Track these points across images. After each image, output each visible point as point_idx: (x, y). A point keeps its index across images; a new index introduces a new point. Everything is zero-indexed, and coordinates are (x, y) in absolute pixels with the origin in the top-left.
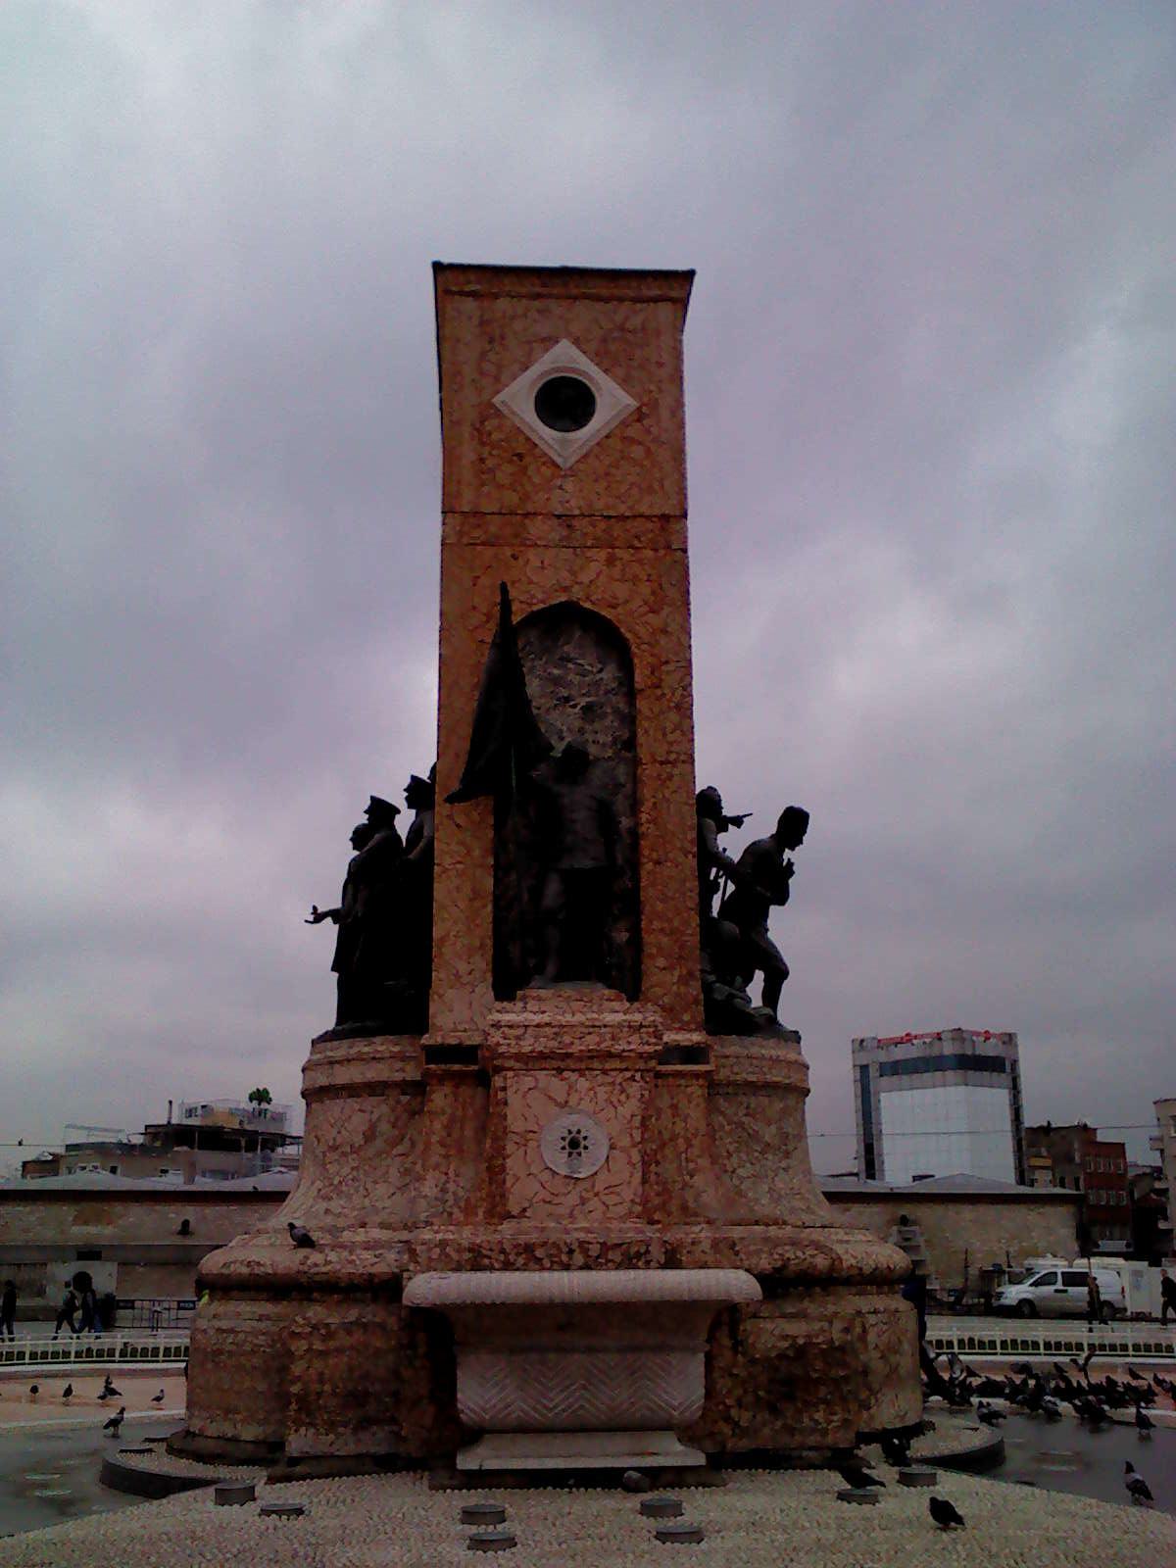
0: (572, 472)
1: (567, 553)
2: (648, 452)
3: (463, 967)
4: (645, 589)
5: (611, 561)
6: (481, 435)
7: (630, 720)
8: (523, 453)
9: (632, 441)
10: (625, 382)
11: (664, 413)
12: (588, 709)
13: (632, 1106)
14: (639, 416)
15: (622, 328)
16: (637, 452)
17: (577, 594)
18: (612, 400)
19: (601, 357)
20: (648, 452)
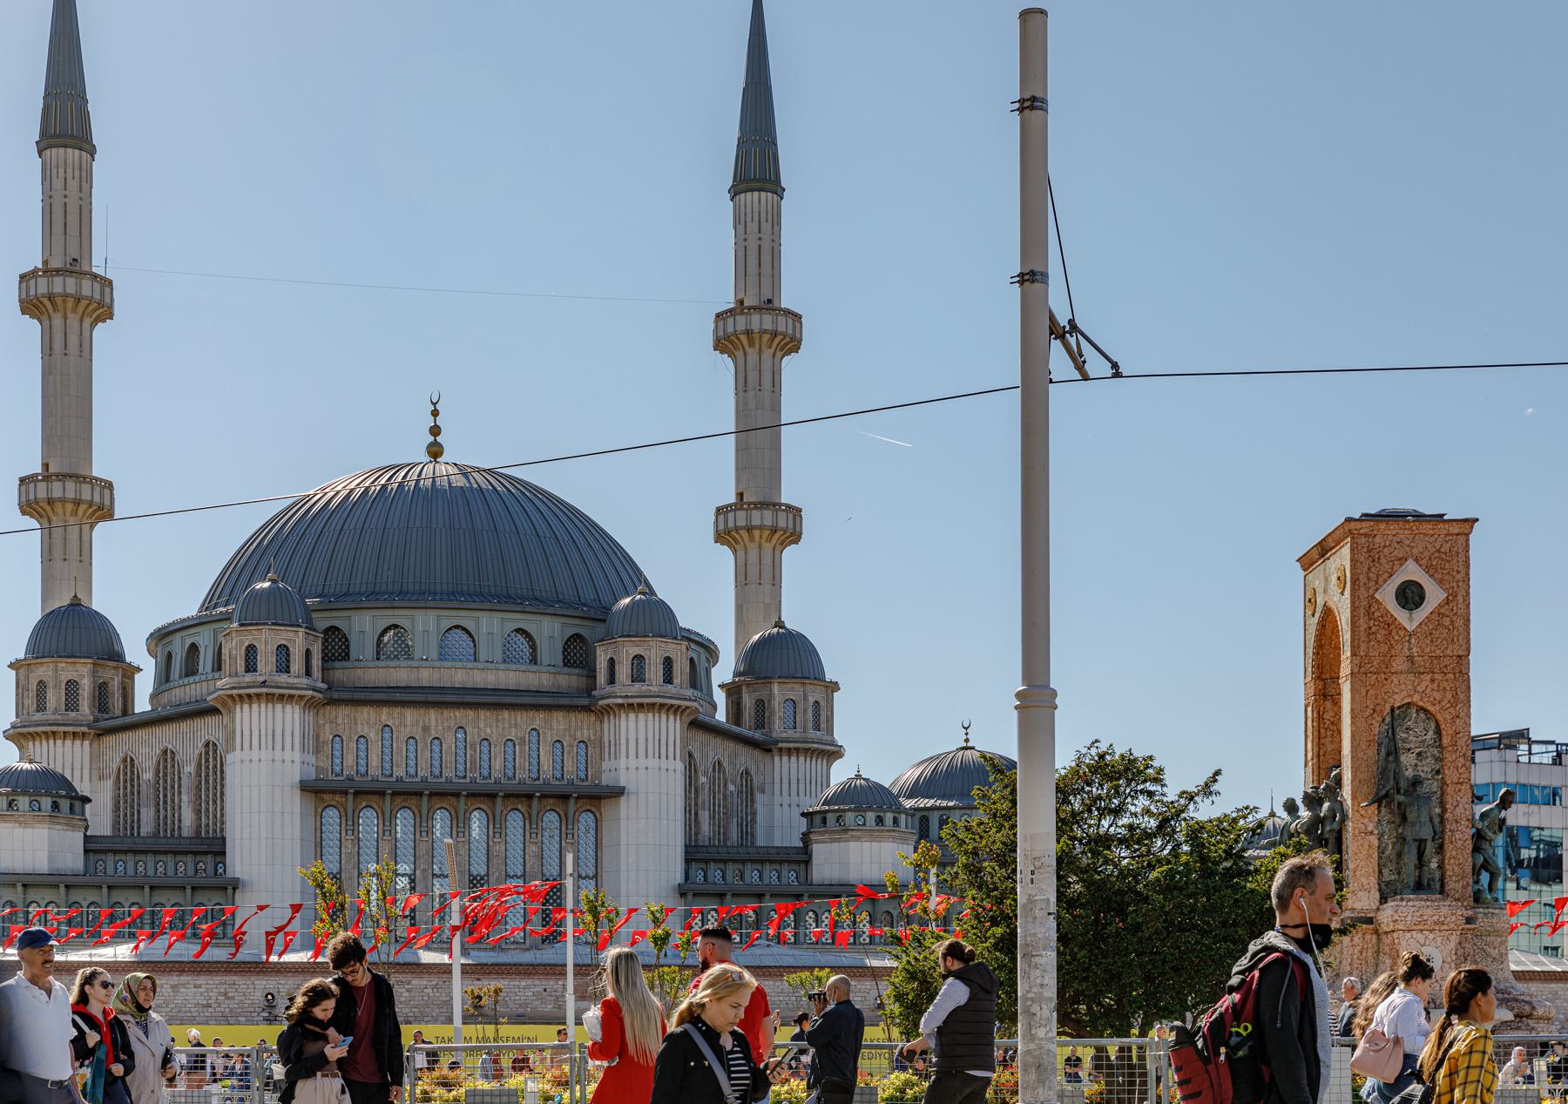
0: (1414, 633)
1: (1411, 677)
2: (1452, 622)
3: (1365, 881)
4: (1449, 695)
5: (1433, 681)
6: (1369, 614)
7: (1439, 760)
8: (1390, 624)
9: (1444, 615)
10: (1440, 582)
11: (1460, 599)
12: (1419, 754)
13: (1452, 945)
14: (1447, 601)
15: (1439, 551)
16: (1446, 622)
17: (1416, 698)
18: (1434, 596)
19: (1429, 570)
20: (1452, 622)
